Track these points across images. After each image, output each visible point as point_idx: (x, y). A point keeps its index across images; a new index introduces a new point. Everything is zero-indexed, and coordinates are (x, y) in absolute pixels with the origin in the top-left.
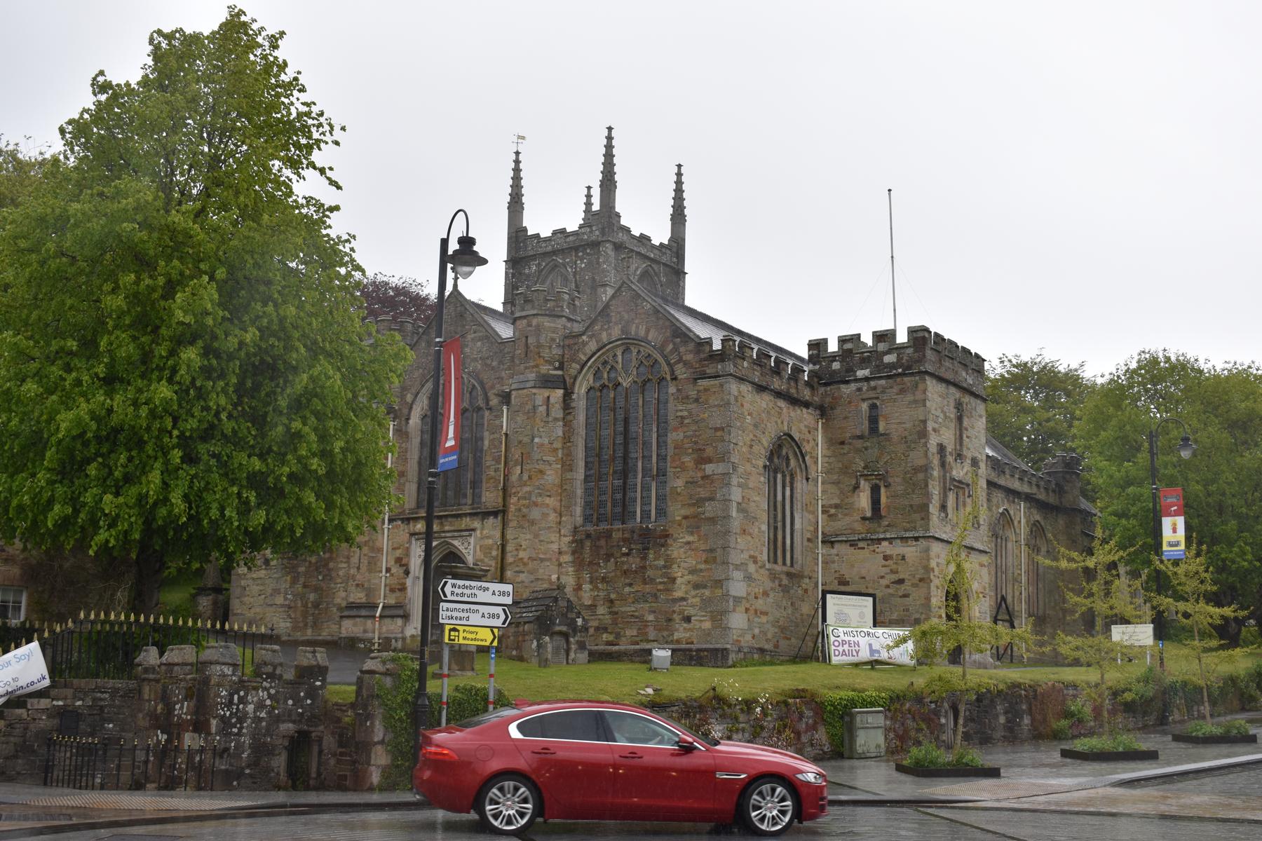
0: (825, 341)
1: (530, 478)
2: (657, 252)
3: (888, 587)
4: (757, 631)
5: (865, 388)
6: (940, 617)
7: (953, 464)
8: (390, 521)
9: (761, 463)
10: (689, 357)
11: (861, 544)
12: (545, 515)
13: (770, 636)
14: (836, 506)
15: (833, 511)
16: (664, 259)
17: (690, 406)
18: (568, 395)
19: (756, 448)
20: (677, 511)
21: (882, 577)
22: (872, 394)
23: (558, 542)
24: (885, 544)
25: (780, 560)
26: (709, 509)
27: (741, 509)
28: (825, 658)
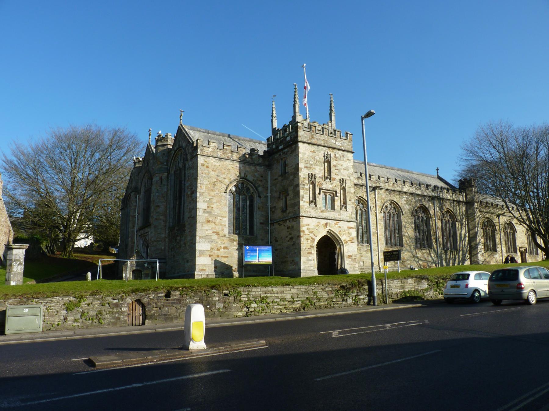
11: (281, 223)
19: (218, 184)
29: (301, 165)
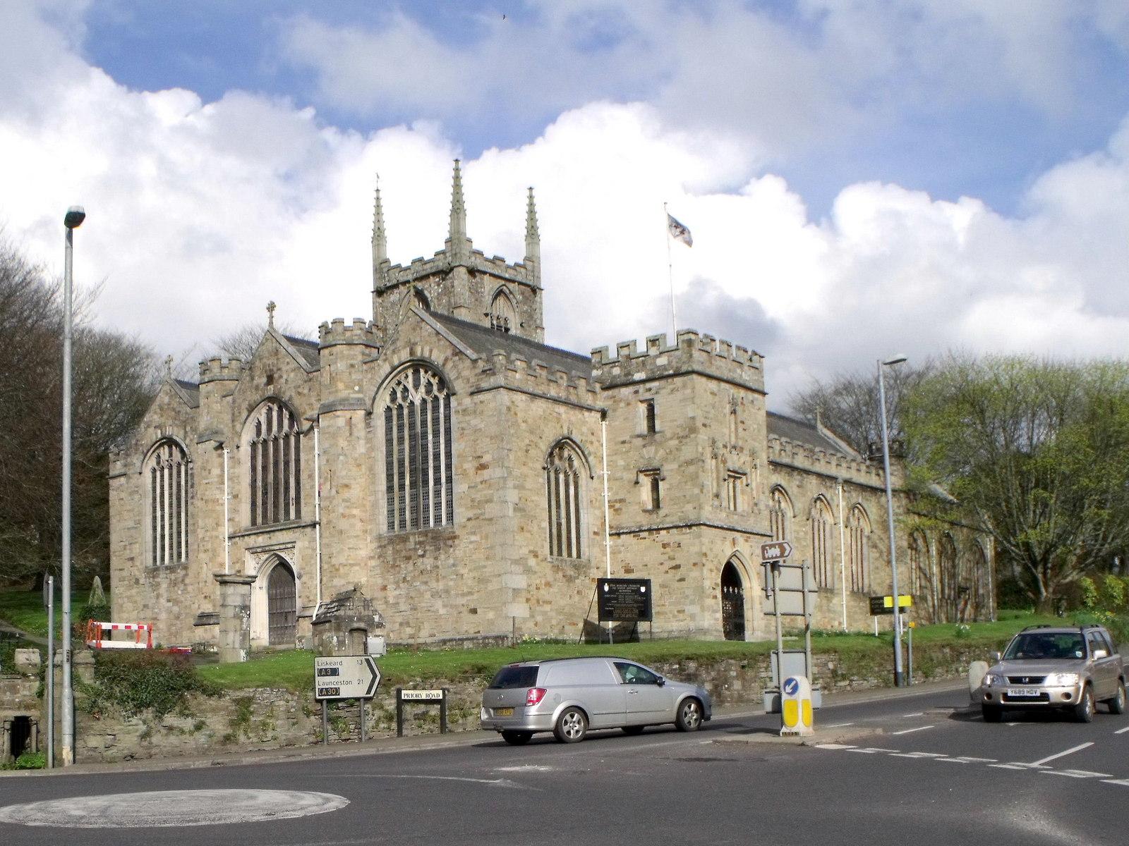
0: (607, 348)
1: (337, 492)
2: (511, 271)
3: (667, 572)
4: (539, 618)
5: (641, 391)
6: (715, 597)
7: (727, 456)
8: (230, 538)
9: (539, 466)
10: (466, 373)
12: (353, 526)
13: (554, 622)
14: (621, 501)
15: (617, 505)
16: (519, 278)
17: (467, 418)
18: (369, 414)
19: (533, 452)
20: (461, 514)
21: (662, 564)
22: (648, 396)
23: (366, 548)
24: (663, 532)
25: (565, 553)
26: (491, 510)
27: (517, 509)
28: (744, 640)
29: (699, 424)
